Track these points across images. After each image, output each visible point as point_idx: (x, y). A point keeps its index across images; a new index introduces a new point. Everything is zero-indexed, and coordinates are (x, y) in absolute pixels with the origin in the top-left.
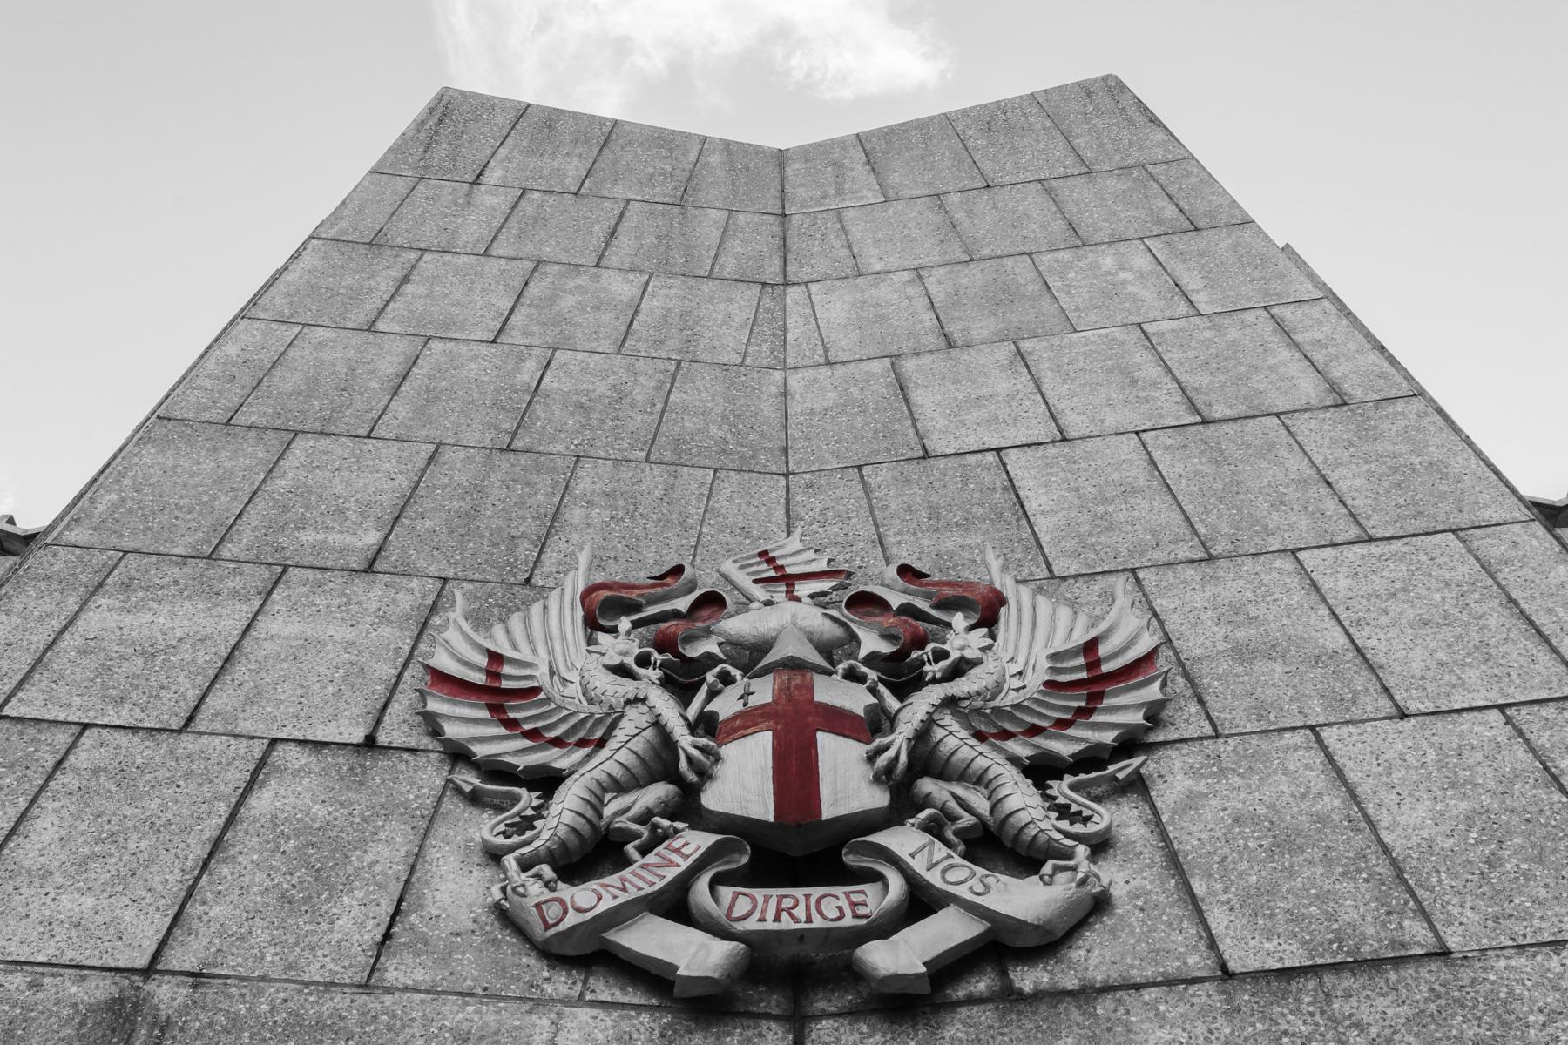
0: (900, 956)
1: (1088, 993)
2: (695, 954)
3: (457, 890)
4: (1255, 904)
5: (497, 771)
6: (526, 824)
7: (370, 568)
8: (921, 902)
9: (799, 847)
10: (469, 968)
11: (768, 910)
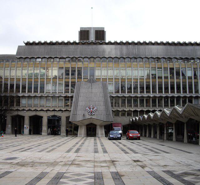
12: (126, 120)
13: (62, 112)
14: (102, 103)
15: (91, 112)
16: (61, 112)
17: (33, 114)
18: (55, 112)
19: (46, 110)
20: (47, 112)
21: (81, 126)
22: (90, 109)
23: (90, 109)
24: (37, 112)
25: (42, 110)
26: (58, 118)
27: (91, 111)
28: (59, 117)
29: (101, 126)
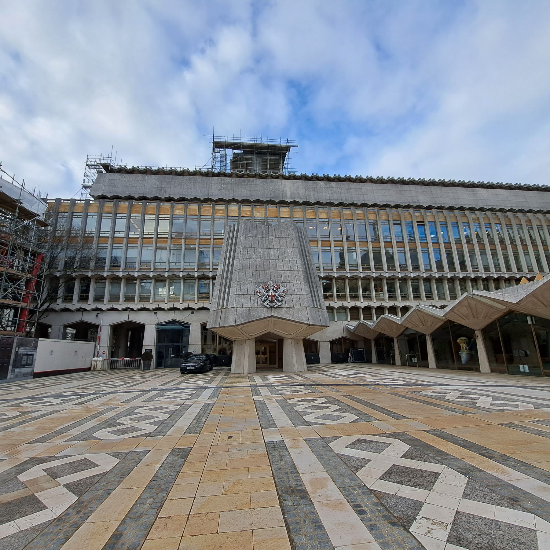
0: (275, 307)
2: (269, 307)
9: (272, 302)
11: (271, 304)
12: (337, 329)
13: (193, 313)
14: (301, 276)
15: (270, 297)
16: (190, 312)
20: (155, 313)
21: (242, 341)
24: (132, 313)
27: (272, 296)
29: (296, 340)
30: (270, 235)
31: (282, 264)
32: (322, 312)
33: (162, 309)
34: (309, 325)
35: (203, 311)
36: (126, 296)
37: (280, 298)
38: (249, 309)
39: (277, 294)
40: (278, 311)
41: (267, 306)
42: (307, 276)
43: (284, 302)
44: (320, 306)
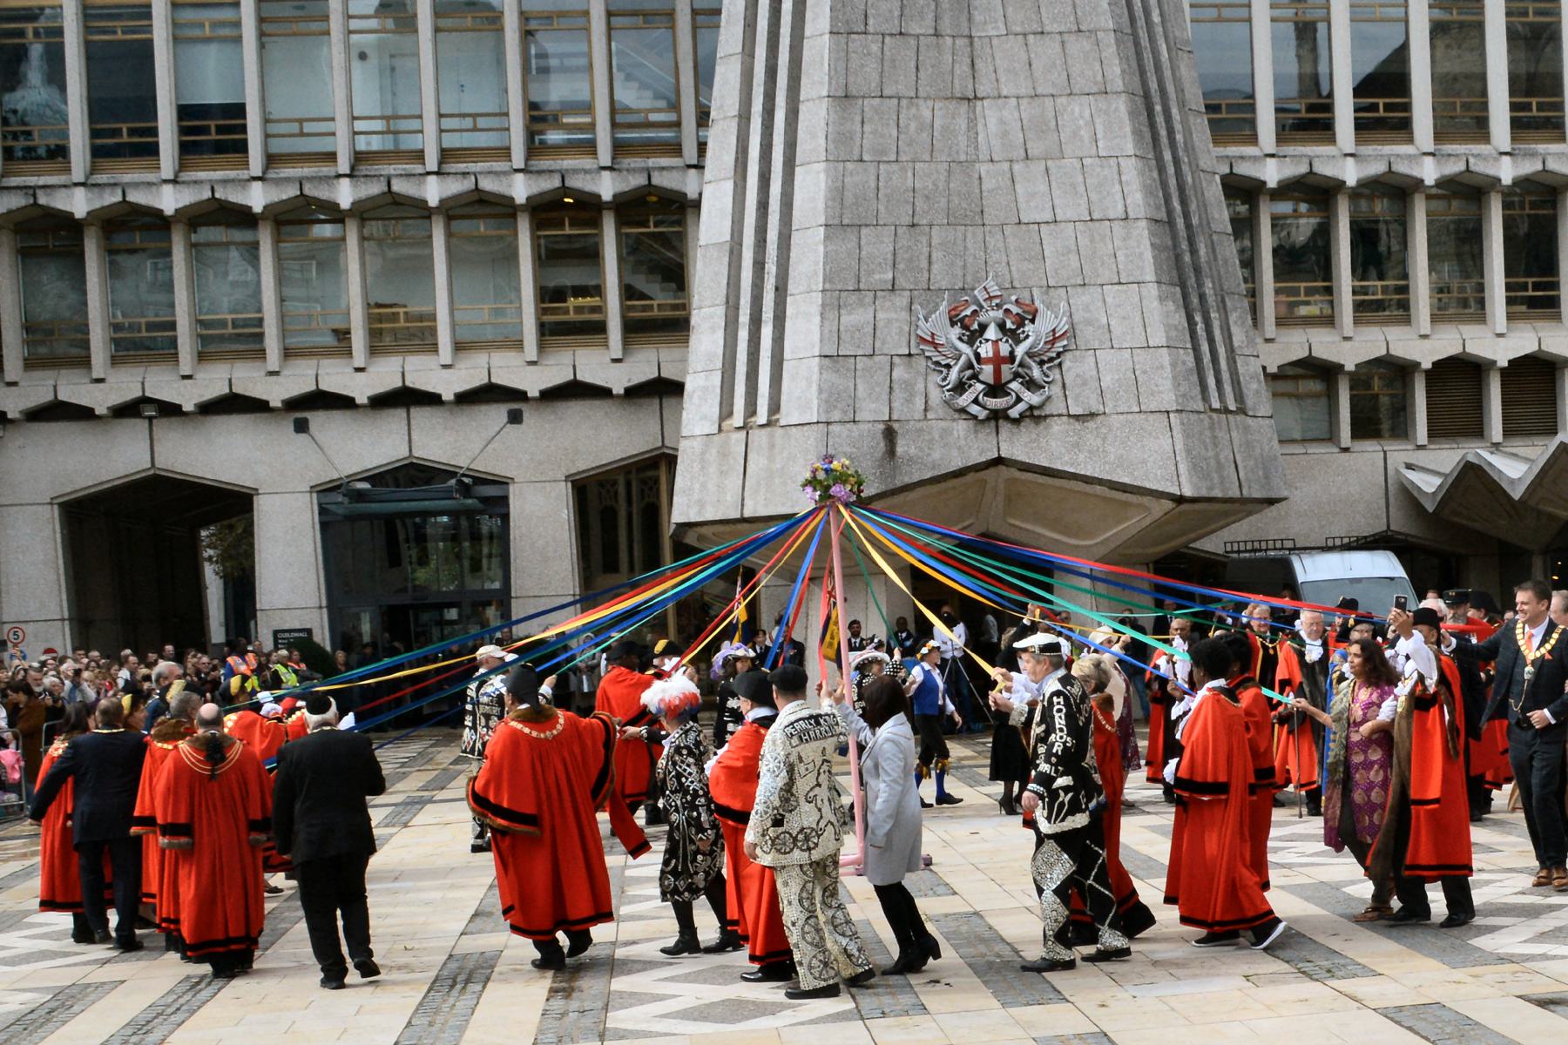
0: (1014, 413)
1: (1046, 417)
2: (982, 414)
3: (936, 396)
4: (1076, 398)
5: (937, 363)
6: (944, 379)
7: (893, 290)
8: (1019, 400)
9: (997, 389)
10: (941, 413)
11: (993, 403)
13: (515, 418)
14: (1138, 250)
15: (987, 371)
16: (496, 414)
17: (121, 457)
18: (420, 415)
19: (293, 405)
20: (301, 427)
22: (974, 336)
23: (974, 336)
25: (233, 404)
26: (465, 490)
27: (997, 361)
28: (480, 481)
30: (978, 17)
31: (1042, 187)
32: (1246, 429)
33: (342, 402)
34: (1180, 500)
35: (575, 410)
36: (117, 327)
37: (1036, 373)
38: (890, 434)
39: (1020, 351)
40: (1028, 431)
41: (974, 409)
42: (1176, 246)
43: (1056, 390)
44: (1240, 397)
